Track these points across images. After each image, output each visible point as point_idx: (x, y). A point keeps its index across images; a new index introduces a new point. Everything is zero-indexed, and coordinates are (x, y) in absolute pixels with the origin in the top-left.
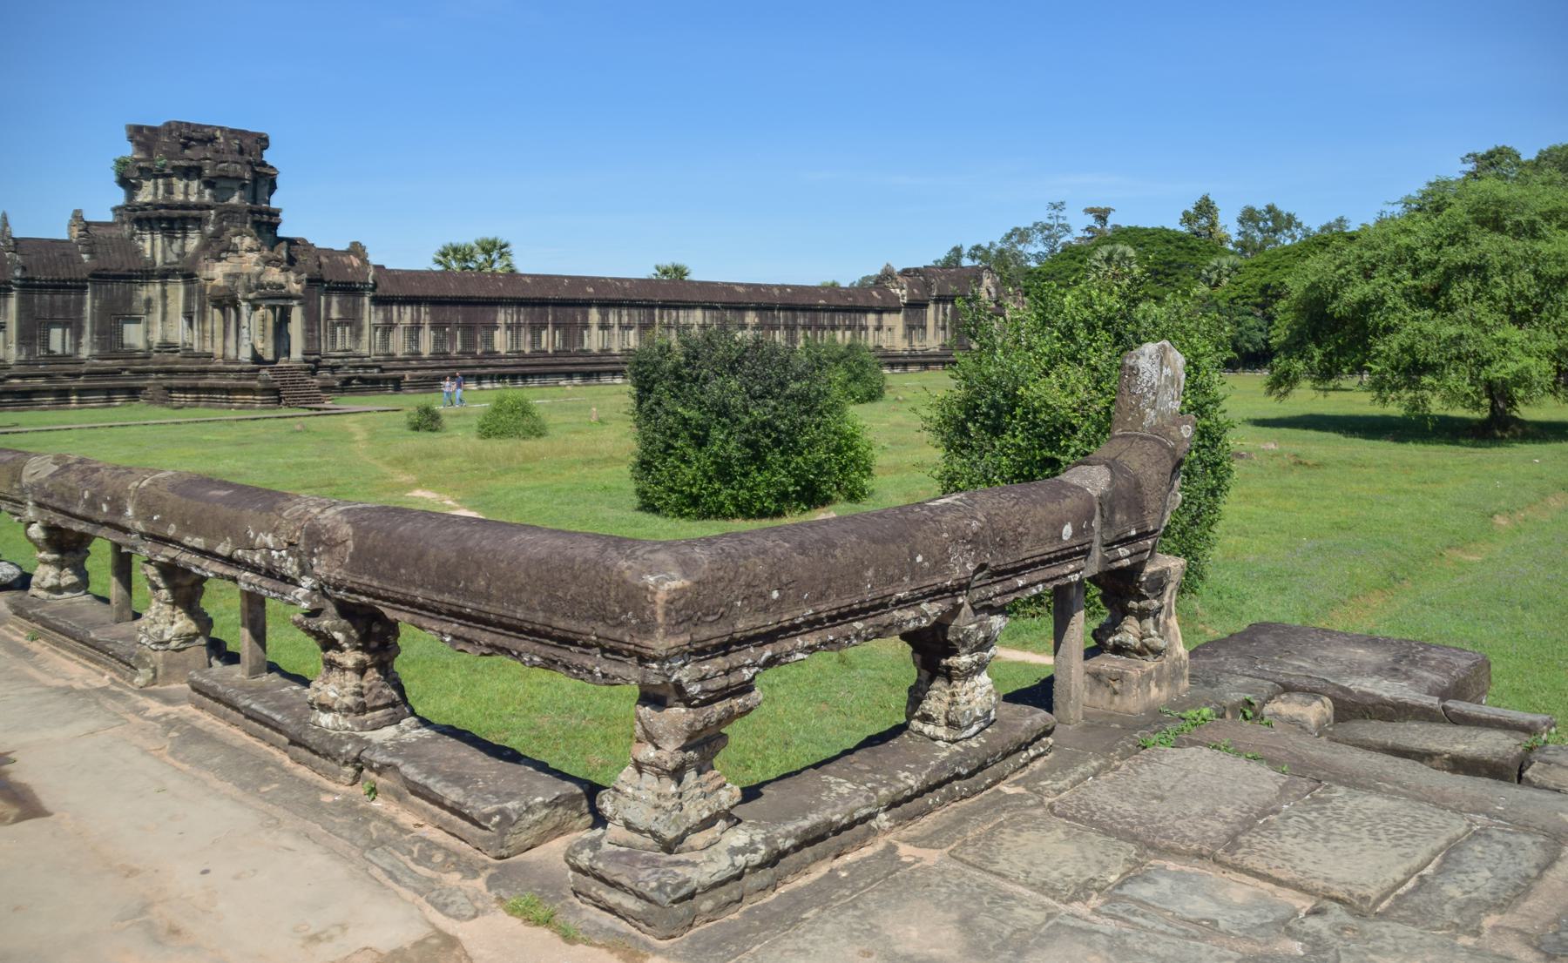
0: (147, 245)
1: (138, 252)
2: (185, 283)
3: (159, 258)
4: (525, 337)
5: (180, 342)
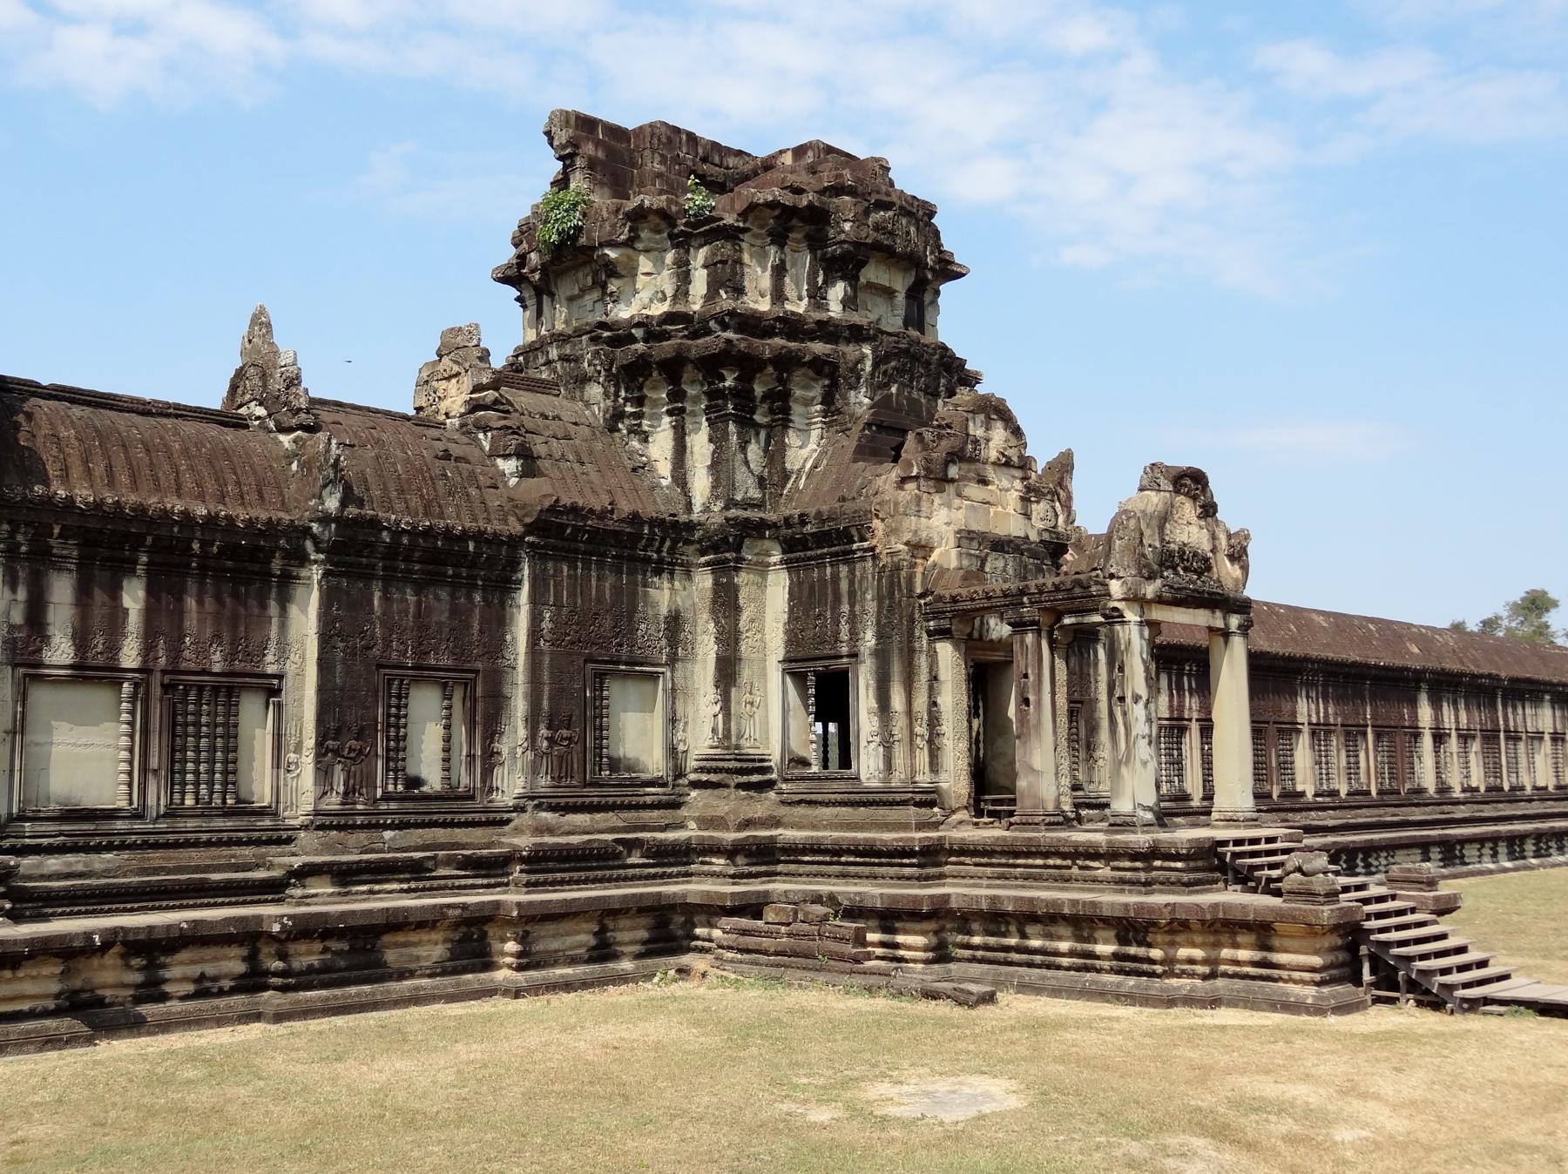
1: (641, 468)
2: (789, 565)
3: (701, 483)
4: (1340, 759)
5: (774, 753)
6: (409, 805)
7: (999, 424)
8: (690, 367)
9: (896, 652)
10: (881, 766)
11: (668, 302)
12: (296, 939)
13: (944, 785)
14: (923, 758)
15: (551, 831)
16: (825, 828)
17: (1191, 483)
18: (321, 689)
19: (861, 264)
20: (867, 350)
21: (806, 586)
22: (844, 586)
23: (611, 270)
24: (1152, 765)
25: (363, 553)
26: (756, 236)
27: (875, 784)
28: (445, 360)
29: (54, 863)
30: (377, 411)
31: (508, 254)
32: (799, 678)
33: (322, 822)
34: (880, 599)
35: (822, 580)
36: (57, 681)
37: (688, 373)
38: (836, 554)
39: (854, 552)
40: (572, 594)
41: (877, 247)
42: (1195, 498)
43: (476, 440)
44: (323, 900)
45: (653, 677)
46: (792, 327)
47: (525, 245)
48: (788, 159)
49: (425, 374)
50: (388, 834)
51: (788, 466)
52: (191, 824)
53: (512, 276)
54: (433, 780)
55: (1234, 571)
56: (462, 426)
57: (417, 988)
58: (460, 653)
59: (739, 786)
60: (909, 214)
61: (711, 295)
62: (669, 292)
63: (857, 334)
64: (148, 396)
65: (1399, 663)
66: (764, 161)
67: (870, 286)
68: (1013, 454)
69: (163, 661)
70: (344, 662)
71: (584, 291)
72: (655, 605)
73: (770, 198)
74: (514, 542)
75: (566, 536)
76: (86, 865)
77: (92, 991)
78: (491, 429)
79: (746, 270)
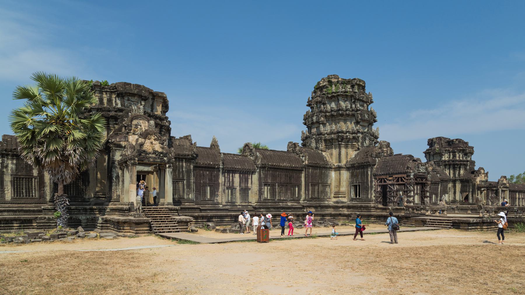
61: (453, 158)
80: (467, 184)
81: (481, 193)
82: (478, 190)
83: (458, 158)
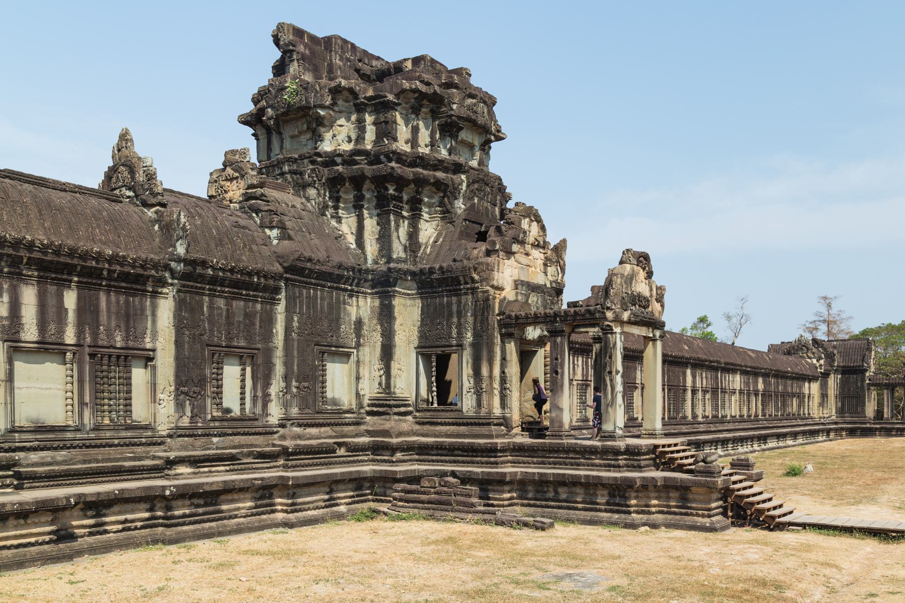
0: (347, 227)
1: (339, 237)
6: (225, 424)
7: (535, 223)
8: (368, 182)
9: (485, 344)
10: (474, 404)
11: (353, 143)
12: (177, 499)
13: (508, 415)
14: (497, 401)
15: (299, 437)
16: (442, 436)
17: (643, 259)
18: (178, 358)
19: (461, 129)
20: (463, 177)
21: (432, 308)
22: (454, 308)
23: (320, 121)
24: (623, 407)
25: (195, 278)
26: (403, 108)
27: (471, 414)
28: (228, 169)
29: (34, 457)
30: (193, 197)
31: (250, 107)
32: (426, 357)
33: (177, 433)
34: (475, 315)
35: (441, 304)
36: (29, 351)
37: (367, 185)
38: (450, 291)
39: (461, 290)
40: (308, 307)
41: (468, 120)
42: (644, 269)
43: (251, 218)
44: (185, 475)
45: (348, 355)
46: (419, 161)
47: (264, 103)
48: (409, 65)
49: (215, 176)
50: (215, 440)
51: (420, 240)
52: (108, 434)
53: (253, 120)
54: (236, 411)
55: (657, 306)
56: (241, 208)
57: (239, 524)
58: (249, 338)
59: (395, 414)
60: (485, 102)
62: (354, 137)
63: (458, 168)
64: (63, 179)
65: (680, 354)
66: (395, 64)
67: (463, 142)
68: (541, 239)
69: (88, 340)
70: (189, 343)
71: (300, 133)
72: (349, 315)
73: (414, 87)
74: (277, 277)
75: (300, 273)
76: (52, 458)
77: (66, 530)
78: (261, 211)
79: (398, 127)
80: (445, 287)
81: (525, 358)
82: (506, 337)
83: (402, 146)
